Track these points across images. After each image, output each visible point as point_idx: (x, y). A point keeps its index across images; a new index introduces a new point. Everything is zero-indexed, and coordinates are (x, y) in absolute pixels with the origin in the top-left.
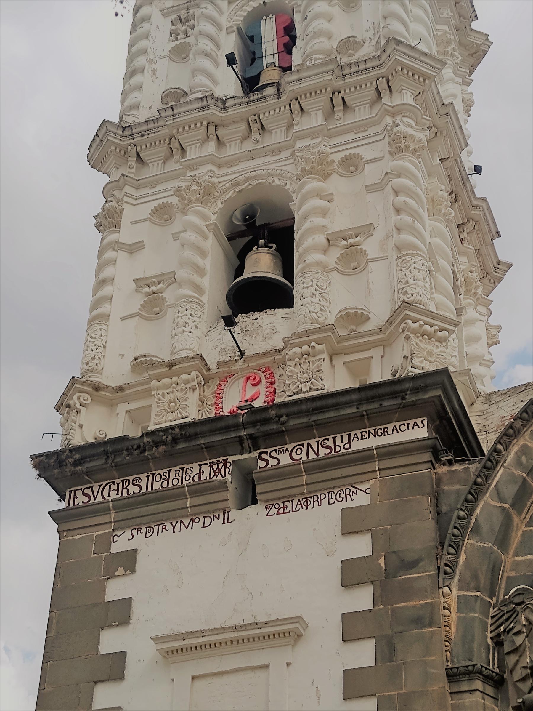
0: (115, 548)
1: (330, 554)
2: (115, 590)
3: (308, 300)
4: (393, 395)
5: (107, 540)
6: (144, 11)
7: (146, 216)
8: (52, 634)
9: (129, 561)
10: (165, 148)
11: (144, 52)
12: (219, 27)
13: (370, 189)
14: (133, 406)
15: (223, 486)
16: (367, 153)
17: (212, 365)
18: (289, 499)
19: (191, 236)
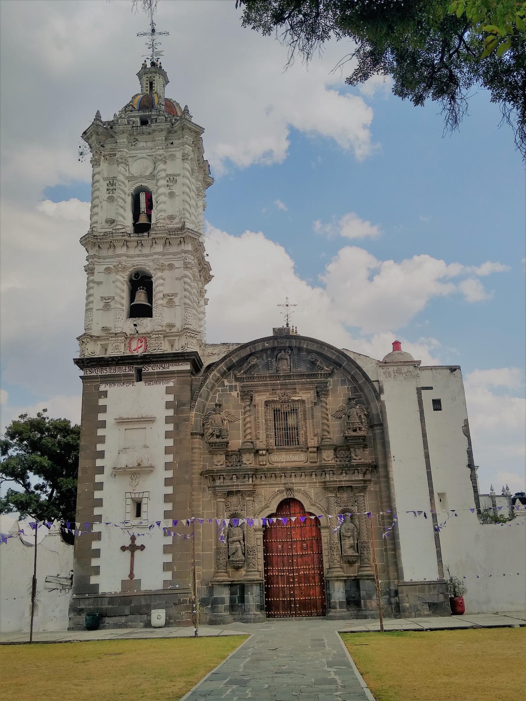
0: (101, 389)
1: (162, 399)
2: (102, 402)
3: (158, 318)
4: (182, 356)
5: (98, 387)
6: (97, 177)
7: (103, 271)
8: (83, 413)
9: (105, 394)
10: (109, 245)
11: (98, 197)
12: (125, 193)
13: (177, 279)
14: (102, 343)
15: (132, 375)
16: (177, 264)
17: (128, 334)
18: (152, 381)
19: (119, 284)
